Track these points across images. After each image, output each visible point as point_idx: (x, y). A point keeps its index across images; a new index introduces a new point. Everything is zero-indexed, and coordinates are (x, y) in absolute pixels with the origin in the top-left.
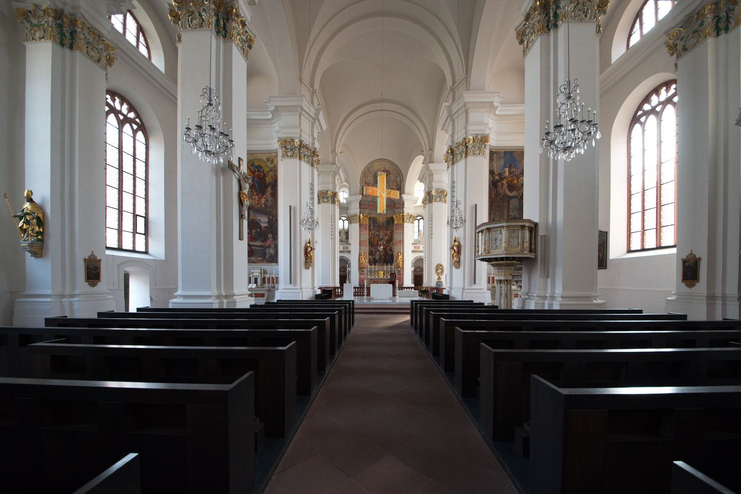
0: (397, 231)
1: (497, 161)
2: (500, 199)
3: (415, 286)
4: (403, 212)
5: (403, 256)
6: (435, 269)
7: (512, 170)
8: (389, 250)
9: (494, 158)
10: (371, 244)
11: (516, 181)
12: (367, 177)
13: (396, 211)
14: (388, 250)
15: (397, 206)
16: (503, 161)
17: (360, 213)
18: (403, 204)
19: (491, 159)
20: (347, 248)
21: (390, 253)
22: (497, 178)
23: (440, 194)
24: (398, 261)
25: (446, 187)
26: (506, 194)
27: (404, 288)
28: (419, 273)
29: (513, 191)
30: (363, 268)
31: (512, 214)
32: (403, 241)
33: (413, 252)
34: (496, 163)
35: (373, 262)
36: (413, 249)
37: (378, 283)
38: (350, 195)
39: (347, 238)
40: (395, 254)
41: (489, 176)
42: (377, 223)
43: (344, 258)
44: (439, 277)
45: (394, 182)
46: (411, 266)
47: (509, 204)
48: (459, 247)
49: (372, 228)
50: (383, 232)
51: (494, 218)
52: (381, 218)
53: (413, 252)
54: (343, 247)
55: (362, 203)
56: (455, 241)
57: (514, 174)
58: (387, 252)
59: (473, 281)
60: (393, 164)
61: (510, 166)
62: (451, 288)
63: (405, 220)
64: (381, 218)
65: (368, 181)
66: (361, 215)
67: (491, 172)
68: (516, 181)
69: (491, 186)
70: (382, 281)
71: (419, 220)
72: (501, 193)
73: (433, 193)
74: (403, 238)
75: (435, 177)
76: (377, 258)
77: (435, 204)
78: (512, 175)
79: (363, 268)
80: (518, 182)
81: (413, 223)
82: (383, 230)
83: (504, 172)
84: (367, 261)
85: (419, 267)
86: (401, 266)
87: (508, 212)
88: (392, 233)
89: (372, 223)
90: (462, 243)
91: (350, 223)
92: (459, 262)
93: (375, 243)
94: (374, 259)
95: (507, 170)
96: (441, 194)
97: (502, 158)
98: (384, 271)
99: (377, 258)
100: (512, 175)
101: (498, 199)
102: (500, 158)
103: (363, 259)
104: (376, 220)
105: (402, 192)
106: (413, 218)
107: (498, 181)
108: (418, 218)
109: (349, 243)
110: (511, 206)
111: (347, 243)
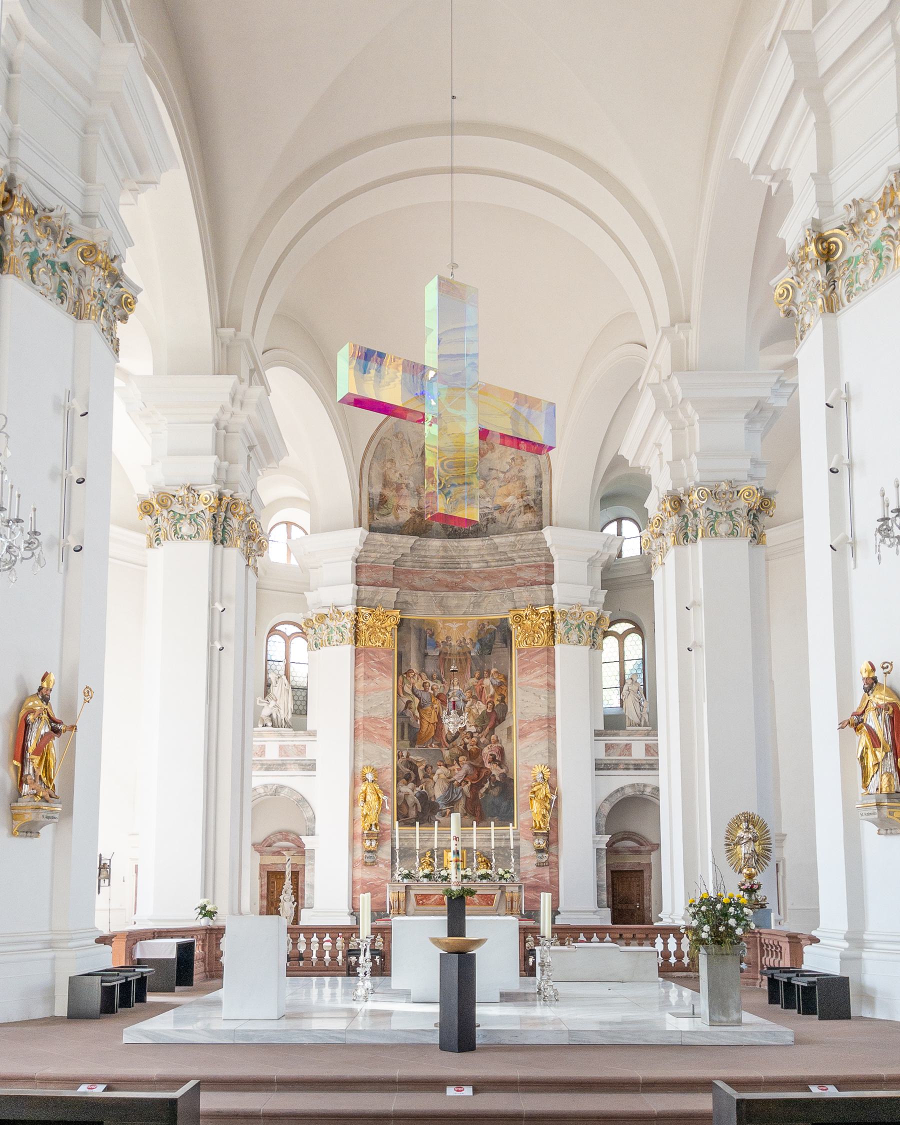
0: (526, 678)
4: (550, 602)
8: (493, 760)
12: (392, 461)
13: (523, 595)
15: (527, 574)
17: (359, 602)
20: (302, 750)
21: (496, 771)
42: (436, 645)
49: (414, 666)
54: (281, 747)
56: (871, 684)
64: (455, 626)
65: (394, 477)
71: (621, 638)
76: (438, 792)
88: (503, 685)
93: (427, 728)
104: (432, 635)
108: (620, 628)
109: (309, 727)
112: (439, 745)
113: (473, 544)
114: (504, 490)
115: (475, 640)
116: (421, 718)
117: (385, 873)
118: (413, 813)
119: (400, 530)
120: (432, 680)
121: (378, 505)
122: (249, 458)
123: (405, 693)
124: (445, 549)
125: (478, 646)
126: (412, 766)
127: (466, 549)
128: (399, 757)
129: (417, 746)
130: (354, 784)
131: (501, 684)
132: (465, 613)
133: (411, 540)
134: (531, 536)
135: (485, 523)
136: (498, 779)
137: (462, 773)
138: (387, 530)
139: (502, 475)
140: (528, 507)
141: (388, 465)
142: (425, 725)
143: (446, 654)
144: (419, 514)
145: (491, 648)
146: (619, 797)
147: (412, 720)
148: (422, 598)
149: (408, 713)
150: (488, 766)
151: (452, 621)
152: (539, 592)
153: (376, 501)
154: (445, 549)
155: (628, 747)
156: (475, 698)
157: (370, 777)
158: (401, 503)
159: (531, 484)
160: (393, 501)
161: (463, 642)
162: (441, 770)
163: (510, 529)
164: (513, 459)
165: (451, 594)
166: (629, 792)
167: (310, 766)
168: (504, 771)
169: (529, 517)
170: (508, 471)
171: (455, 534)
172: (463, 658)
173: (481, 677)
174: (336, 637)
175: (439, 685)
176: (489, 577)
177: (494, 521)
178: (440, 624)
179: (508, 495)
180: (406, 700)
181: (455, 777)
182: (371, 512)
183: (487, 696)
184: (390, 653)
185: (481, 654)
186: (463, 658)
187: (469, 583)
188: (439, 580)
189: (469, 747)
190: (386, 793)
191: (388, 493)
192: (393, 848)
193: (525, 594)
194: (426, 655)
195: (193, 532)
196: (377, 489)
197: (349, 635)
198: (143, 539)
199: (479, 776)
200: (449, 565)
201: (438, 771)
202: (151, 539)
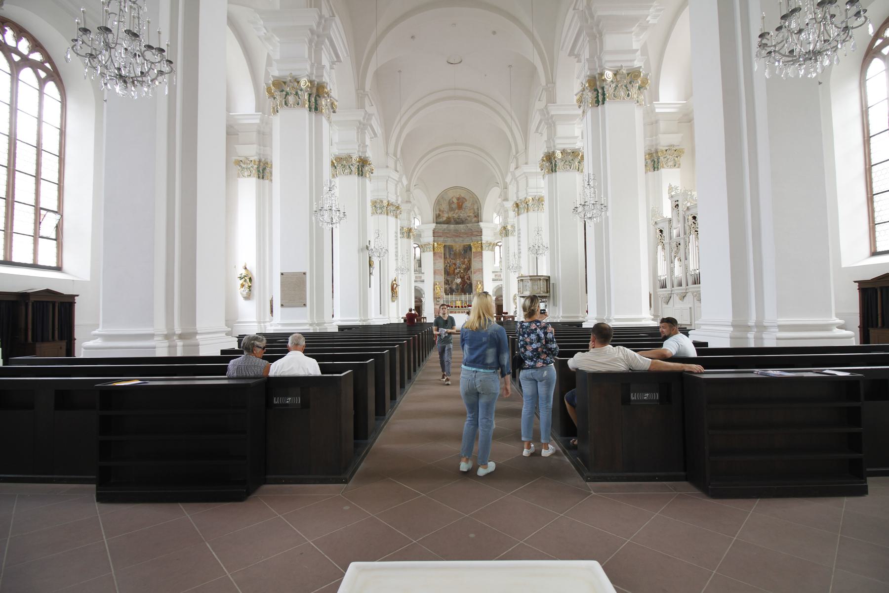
0: (476, 259)
4: (481, 240)
5: (482, 285)
8: (467, 279)
10: (447, 273)
12: (441, 205)
13: (474, 238)
14: (466, 279)
20: (421, 277)
21: (468, 282)
24: (478, 290)
25: (544, 193)
28: (498, 302)
30: (439, 298)
32: (482, 269)
33: (494, 280)
35: (449, 291)
36: (494, 277)
39: (420, 266)
40: (474, 283)
42: (453, 251)
45: (470, 210)
49: (448, 256)
52: (457, 246)
53: (494, 280)
60: (468, 191)
65: (442, 209)
66: (435, 244)
74: (482, 266)
76: (454, 287)
79: (439, 298)
81: (493, 250)
84: (443, 290)
89: (447, 250)
91: (422, 251)
93: (451, 272)
94: (450, 288)
98: (462, 301)
99: (454, 287)
103: (438, 289)
111: (420, 272)
112: (454, 275)
113: (461, 226)
114: (469, 212)
118: (448, 292)
119: (444, 223)
121: (438, 216)
124: (455, 227)
130: (434, 285)
133: (446, 225)
134: (476, 224)
140: (475, 216)
144: (449, 218)
145: (466, 251)
146: (498, 287)
148: (449, 239)
152: (479, 238)
153: (438, 215)
154: (455, 227)
157: (438, 284)
158: (444, 215)
159: (476, 210)
160: (442, 215)
161: (459, 250)
163: (471, 222)
167: (423, 281)
169: (476, 219)
171: (457, 223)
173: (464, 259)
174: (428, 250)
175: (454, 261)
176: (466, 234)
177: (467, 219)
182: (436, 218)
183: (466, 263)
184: (442, 253)
185: (464, 253)
187: (461, 236)
191: (440, 213)
196: (438, 212)
199: (463, 282)
200: (456, 231)
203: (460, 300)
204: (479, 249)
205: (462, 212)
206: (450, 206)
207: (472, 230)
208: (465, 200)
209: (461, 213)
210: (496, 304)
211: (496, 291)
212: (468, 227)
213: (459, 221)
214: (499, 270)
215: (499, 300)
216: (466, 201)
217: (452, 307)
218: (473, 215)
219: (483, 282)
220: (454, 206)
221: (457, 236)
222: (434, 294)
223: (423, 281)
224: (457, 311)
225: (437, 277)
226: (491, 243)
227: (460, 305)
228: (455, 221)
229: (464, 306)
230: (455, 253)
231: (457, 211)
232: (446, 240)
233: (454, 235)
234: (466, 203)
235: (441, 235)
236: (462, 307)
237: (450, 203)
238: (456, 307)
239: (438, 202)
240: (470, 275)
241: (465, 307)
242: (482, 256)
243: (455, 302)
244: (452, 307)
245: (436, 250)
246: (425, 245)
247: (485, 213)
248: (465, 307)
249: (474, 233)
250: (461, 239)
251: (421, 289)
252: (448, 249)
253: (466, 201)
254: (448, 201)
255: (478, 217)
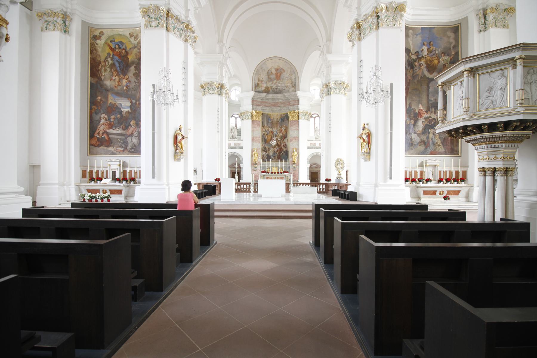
1: (413, 38)
2: (418, 81)
3: (311, 182)
4: (298, 109)
5: (298, 153)
6: (334, 164)
7: (431, 49)
8: (284, 147)
9: (410, 34)
11: (436, 62)
12: (260, 75)
13: (291, 107)
16: (420, 38)
17: (253, 109)
18: (298, 101)
19: (407, 36)
20: (239, 144)
21: (284, 149)
22: (414, 57)
23: (339, 86)
24: (293, 157)
26: (425, 76)
27: (300, 184)
29: (433, 72)
30: (256, 164)
31: (432, 99)
32: (298, 137)
33: (309, 148)
34: (412, 41)
35: (267, 158)
36: (309, 145)
37: (271, 179)
38: (242, 91)
40: (290, 150)
41: (405, 54)
42: (271, 120)
43: (235, 154)
44: (339, 172)
46: (307, 163)
47: (428, 88)
48: (369, 136)
50: (277, 128)
51: (410, 103)
52: (275, 115)
53: (309, 148)
54: (235, 143)
55: (255, 99)
57: (434, 52)
58: (282, 148)
59: (389, 176)
61: (430, 43)
62: (358, 184)
63: (300, 116)
64: (275, 115)
65: (261, 79)
66: (254, 112)
67: (408, 51)
68: (436, 62)
69: (407, 67)
70: (276, 177)
71: (315, 118)
72: (418, 75)
73: (332, 85)
74: (298, 135)
75: (334, 69)
76: (271, 154)
77: (333, 97)
78: (431, 54)
79: (256, 164)
80: (439, 62)
81: (308, 120)
82: (277, 126)
83: (422, 51)
84: (260, 157)
85: (315, 164)
86: (296, 162)
87: (428, 96)
88: (286, 130)
90: (373, 131)
92: (369, 152)
94: (268, 155)
95: (425, 48)
96: (342, 86)
97: (419, 34)
99: (271, 154)
100: (431, 54)
101: (416, 81)
102: (417, 35)
103: (256, 155)
104: (270, 117)
105: (297, 89)
106: (309, 116)
107: (415, 61)
108: (314, 116)
110: (430, 90)
113: (279, 96)
115: (280, 118)
116: (267, 137)
117: (259, 172)
120: (270, 128)
121: (257, 86)
122: (226, 74)
123: (263, 131)
124: (273, 96)
125: (281, 120)
126: (265, 148)
127: (278, 96)
128: (262, 146)
129: (266, 144)
131: (286, 129)
132: (278, 112)
134: (293, 93)
135: (282, 90)
136: (285, 151)
137: (277, 150)
138: (259, 92)
139: (286, 78)
141: (259, 76)
142: (268, 139)
143: (273, 122)
144: (267, 88)
145: (284, 120)
146: (313, 155)
147: (265, 137)
148: (267, 109)
149: (264, 136)
150: (283, 148)
151: (274, 114)
152: (295, 107)
153: (257, 84)
155: (315, 144)
156: (280, 132)
157: (255, 150)
158: (262, 85)
159: (293, 80)
160: (260, 85)
162: (272, 149)
163: (288, 91)
164: (289, 74)
165: (274, 107)
166: (315, 154)
167: (242, 148)
168: (286, 149)
169: (293, 89)
170: (288, 77)
171: (275, 93)
172: (277, 123)
173: (281, 127)
174: (247, 118)
175: (272, 129)
176: (284, 103)
177: (285, 89)
178: (272, 115)
179: (288, 83)
180: (264, 133)
181: (275, 151)
184: (260, 121)
185: (281, 122)
186: (277, 123)
187: (278, 105)
188: (272, 104)
189: (278, 144)
190: (259, 154)
191: (259, 83)
192: (261, 167)
193: (292, 108)
194: (268, 122)
195: (213, 92)
196: (257, 82)
197: (250, 117)
198: (201, 94)
199: (280, 150)
200: (274, 100)
201: (271, 149)
202: (203, 94)
203: (276, 167)
204: (296, 118)
205: (280, 82)
206: (268, 76)
207: (289, 99)
208: (283, 71)
209: (279, 83)
210: (310, 171)
211: (311, 158)
212: (285, 96)
213: (277, 91)
214: (314, 139)
215: (312, 168)
216: (284, 71)
217: (268, 173)
218: (291, 85)
219: (298, 149)
220: (272, 76)
221: (275, 106)
222: (252, 160)
223: (242, 148)
224: (273, 177)
225: (255, 143)
226: (307, 112)
227: (276, 172)
228: (273, 91)
229: (280, 172)
230: (272, 122)
231: (275, 81)
232: (264, 108)
233: (272, 105)
234: (284, 73)
235: (260, 104)
236: (278, 173)
237: (269, 73)
238: (272, 173)
239: (257, 72)
240: (286, 143)
241: (281, 173)
242: (298, 124)
243: (272, 169)
244: (268, 173)
245: (254, 118)
246: (244, 113)
247: (303, 83)
248: (281, 173)
249: (290, 103)
250: (278, 108)
251: (240, 156)
252: (266, 118)
253: (284, 71)
254: (266, 72)
255: (295, 86)
